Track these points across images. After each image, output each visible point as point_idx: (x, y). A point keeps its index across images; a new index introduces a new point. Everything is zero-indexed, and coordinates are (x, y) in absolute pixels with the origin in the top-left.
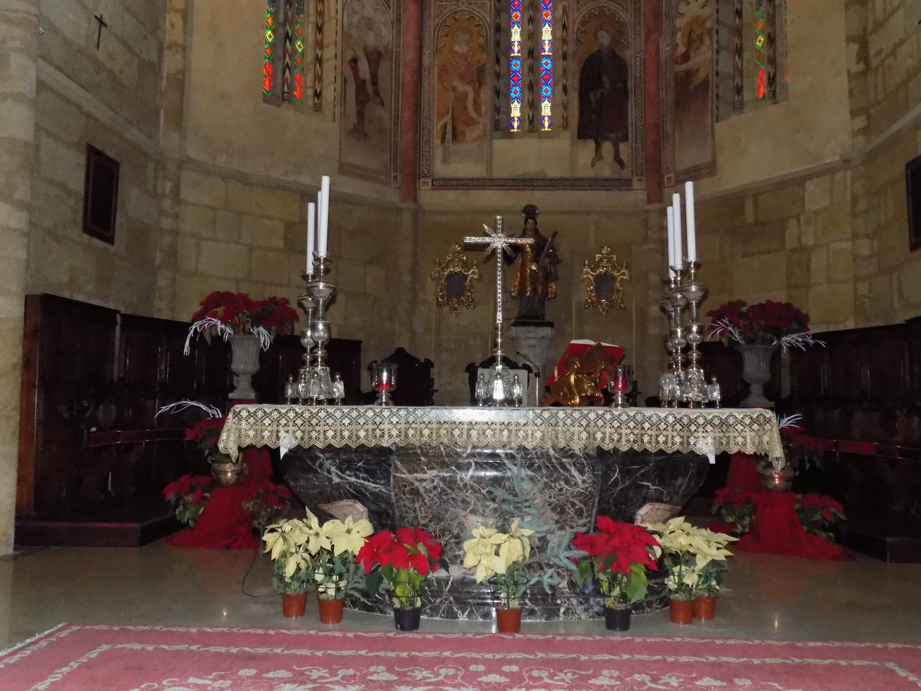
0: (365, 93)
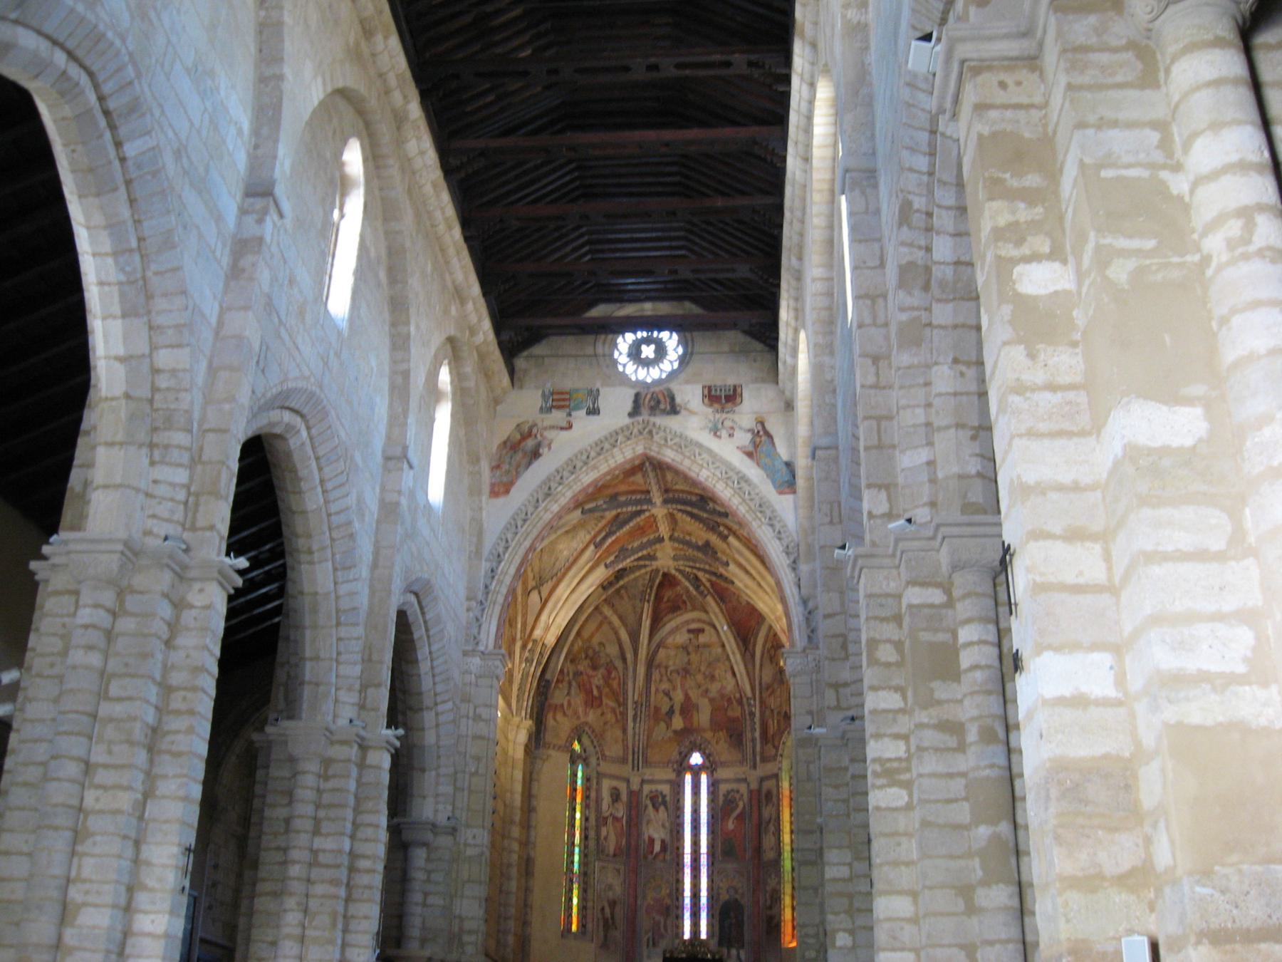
0: (608, 925)
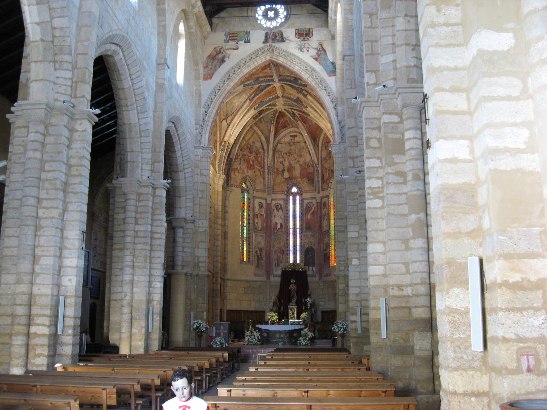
0: (259, 258)
